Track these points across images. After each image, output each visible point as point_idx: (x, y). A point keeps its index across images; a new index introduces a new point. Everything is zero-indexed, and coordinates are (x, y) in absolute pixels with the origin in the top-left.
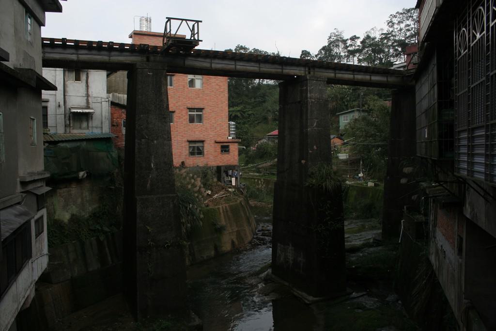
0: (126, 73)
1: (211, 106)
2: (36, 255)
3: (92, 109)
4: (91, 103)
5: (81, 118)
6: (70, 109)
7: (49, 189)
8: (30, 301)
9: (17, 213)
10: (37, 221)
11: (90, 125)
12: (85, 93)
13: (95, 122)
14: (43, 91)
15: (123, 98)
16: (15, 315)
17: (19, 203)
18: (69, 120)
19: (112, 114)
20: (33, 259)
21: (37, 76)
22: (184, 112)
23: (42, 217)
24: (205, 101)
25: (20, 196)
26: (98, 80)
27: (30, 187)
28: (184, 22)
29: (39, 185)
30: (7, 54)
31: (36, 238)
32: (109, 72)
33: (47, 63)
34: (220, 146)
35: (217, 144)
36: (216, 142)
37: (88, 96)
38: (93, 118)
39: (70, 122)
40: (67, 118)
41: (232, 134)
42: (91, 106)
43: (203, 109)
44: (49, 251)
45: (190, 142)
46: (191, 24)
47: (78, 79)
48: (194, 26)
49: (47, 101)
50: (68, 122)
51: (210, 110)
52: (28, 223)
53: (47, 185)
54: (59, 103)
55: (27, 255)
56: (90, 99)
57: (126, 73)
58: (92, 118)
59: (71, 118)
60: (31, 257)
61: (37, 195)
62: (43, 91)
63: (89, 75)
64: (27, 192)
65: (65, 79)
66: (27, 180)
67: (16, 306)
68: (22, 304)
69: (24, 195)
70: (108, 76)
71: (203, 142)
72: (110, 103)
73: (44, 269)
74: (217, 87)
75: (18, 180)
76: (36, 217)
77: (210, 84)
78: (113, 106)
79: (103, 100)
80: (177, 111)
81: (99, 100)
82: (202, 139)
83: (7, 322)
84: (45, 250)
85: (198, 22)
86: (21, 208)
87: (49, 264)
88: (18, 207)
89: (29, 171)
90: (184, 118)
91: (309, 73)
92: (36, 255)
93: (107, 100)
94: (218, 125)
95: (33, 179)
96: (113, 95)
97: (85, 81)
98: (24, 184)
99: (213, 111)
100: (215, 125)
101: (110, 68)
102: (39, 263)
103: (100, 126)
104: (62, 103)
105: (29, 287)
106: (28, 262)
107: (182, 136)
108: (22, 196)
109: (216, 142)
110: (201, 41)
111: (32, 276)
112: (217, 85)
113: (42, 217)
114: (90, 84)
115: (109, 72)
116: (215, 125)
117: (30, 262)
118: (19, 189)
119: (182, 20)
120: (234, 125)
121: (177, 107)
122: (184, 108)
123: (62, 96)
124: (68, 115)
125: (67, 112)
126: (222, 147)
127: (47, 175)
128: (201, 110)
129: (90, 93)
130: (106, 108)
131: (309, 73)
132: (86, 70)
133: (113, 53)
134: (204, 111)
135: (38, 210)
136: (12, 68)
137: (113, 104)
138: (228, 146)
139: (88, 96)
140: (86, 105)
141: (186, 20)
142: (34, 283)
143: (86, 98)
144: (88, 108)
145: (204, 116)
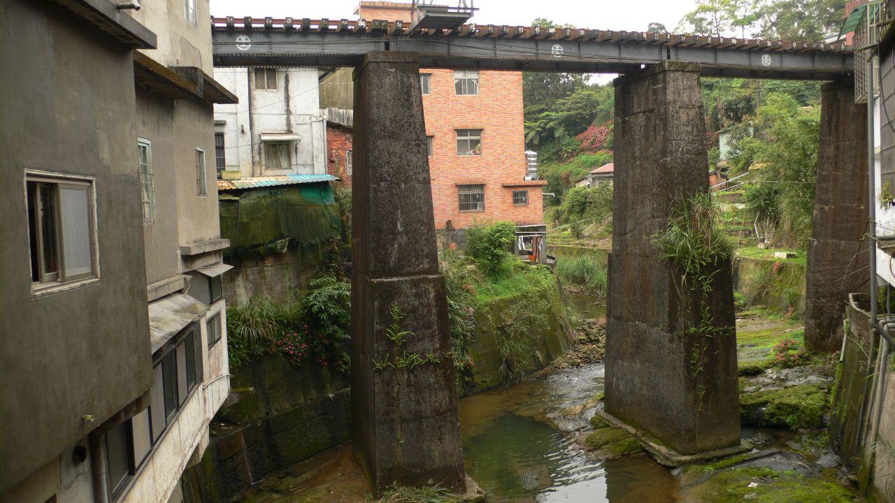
0: (350, 70)
1: (494, 126)
2: (210, 377)
3: (297, 134)
5: (278, 150)
6: (260, 136)
7: (228, 267)
8: (202, 452)
9: (177, 307)
10: (210, 322)
11: (294, 161)
12: (285, 108)
13: (301, 157)
14: (215, 105)
15: (347, 114)
16: (179, 476)
17: (180, 292)
18: (260, 153)
19: (329, 142)
20: (206, 382)
21: (204, 80)
22: (449, 136)
23: (218, 314)
24: (485, 117)
25: (182, 281)
26: (305, 85)
27: (198, 265)
29: (212, 260)
30: (154, 36)
31: (209, 349)
32: (322, 73)
33: (221, 61)
34: (511, 193)
35: (505, 191)
36: (505, 187)
37: (288, 112)
38: (299, 150)
39: (260, 158)
40: (256, 152)
41: (532, 172)
42: (293, 129)
43: (481, 130)
44: (231, 371)
45: (460, 187)
47: (272, 85)
49: (222, 124)
50: (257, 158)
51: (494, 131)
52: (194, 324)
53: (225, 262)
54: (242, 126)
55: (195, 376)
56: (292, 118)
57: (350, 70)
58: (296, 150)
59: (263, 151)
60: (202, 380)
61: (209, 278)
62: (215, 105)
63: (290, 78)
64: (195, 273)
65: (252, 86)
66: (192, 254)
67: (179, 462)
68: (188, 458)
69: (189, 277)
70: (321, 78)
71: (482, 186)
72: (325, 124)
73: (223, 400)
74: (505, 92)
75: (179, 252)
76: (209, 314)
77: (493, 87)
78: (330, 129)
79: (314, 119)
80: (438, 135)
81: (307, 119)
82: (480, 182)
83: (165, 488)
84: (225, 370)
86: (184, 300)
87: (231, 393)
88: (179, 297)
89: (194, 237)
90: (449, 146)
91: (669, 57)
92: (210, 377)
93: (321, 119)
94: (507, 157)
95: (202, 252)
96: (330, 112)
98: (188, 258)
99: (498, 134)
100: (503, 158)
101: (325, 65)
102: (213, 392)
103: (309, 162)
105: (200, 430)
106: (197, 388)
107: (447, 177)
108: (185, 279)
109: (505, 187)
111: (205, 411)
112: (504, 88)
113: (218, 314)
114: (291, 94)
115: (322, 73)
116: (503, 158)
117: (201, 388)
118: (180, 267)
120: (534, 156)
121: (437, 128)
122: (450, 130)
125: (257, 141)
126: (515, 195)
127: (226, 244)
128: (478, 131)
129: (292, 109)
130: (319, 131)
131: (669, 57)
132: (286, 70)
133: (328, 39)
134: (483, 135)
135: (212, 303)
136: (166, 66)
137: (331, 126)
138: (525, 193)
139: (288, 112)
140: (286, 128)
142: (207, 424)
143: (285, 116)
144: (289, 132)
145: (483, 141)
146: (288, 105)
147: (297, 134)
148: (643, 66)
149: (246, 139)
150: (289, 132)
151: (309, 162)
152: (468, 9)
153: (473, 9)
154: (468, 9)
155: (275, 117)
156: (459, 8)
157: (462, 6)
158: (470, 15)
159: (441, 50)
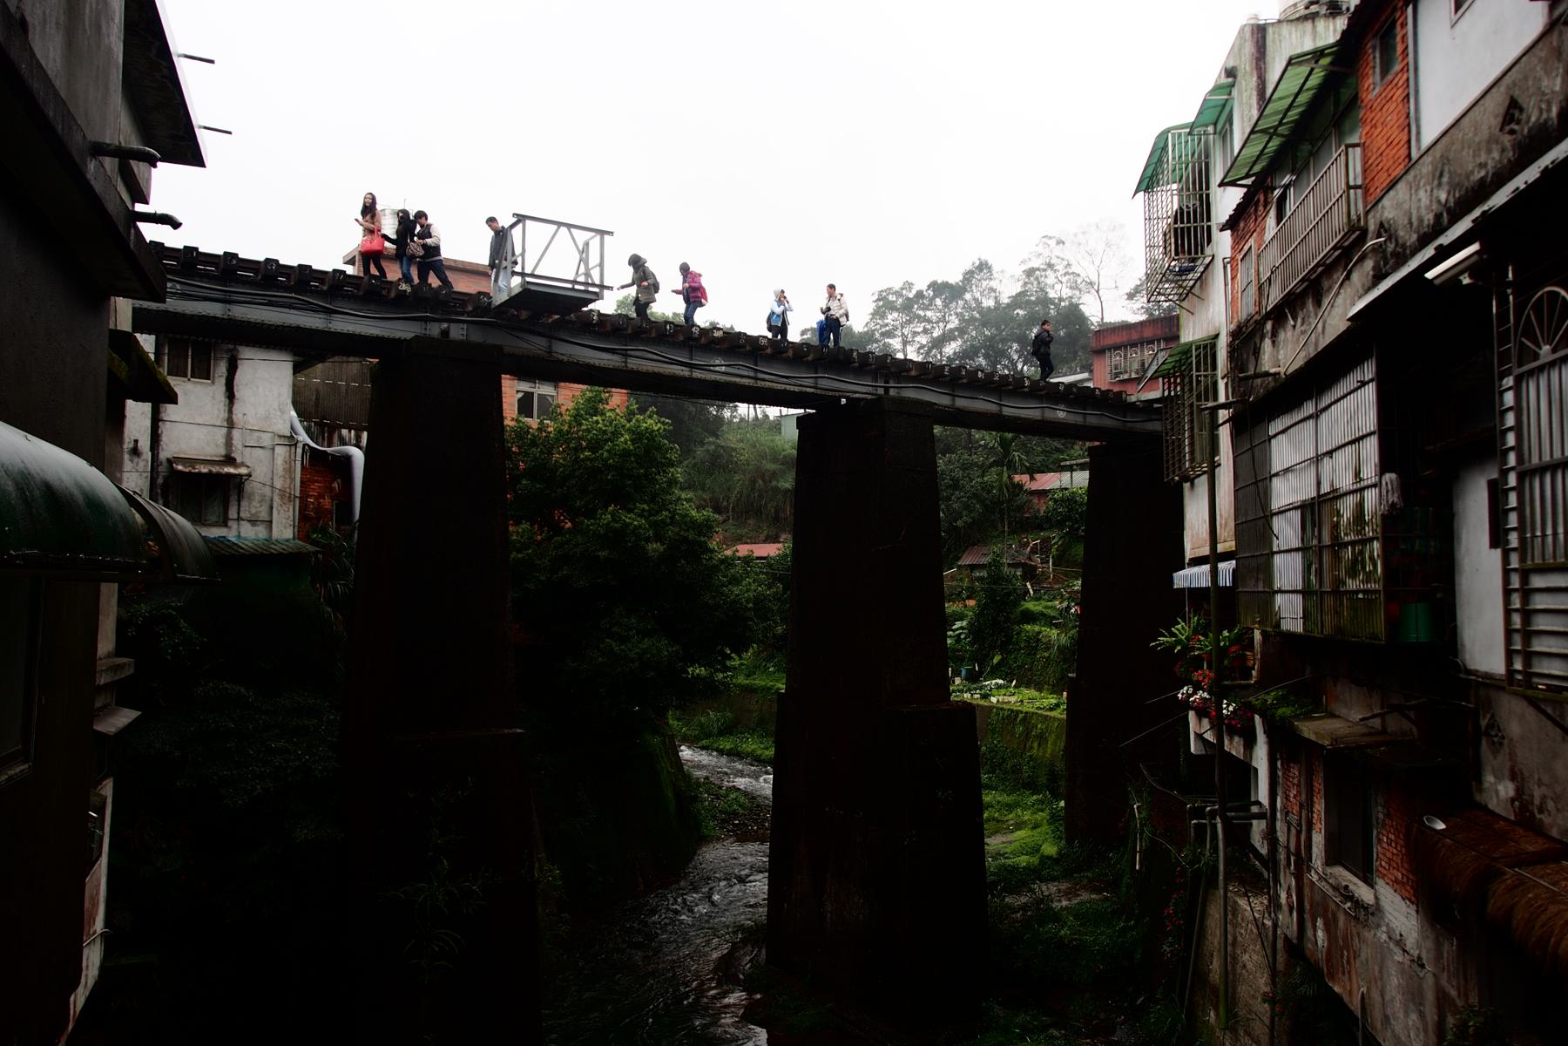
3: (243, 464)
4: (240, 446)
11: (233, 513)
13: (251, 508)
14: (129, 403)
28: (563, 230)
37: (231, 424)
46: (582, 237)
47: (203, 373)
48: (587, 244)
54: (136, 441)
56: (236, 434)
62: (129, 403)
70: (297, 369)
72: (299, 451)
81: (266, 440)
85: (602, 233)
97: (223, 381)
101: (304, 349)
103: (264, 515)
104: (145, 444)
110: (677, 292)
119: (560, 224)
123: (148, 423)
124: (160, 481)
139: (231, 424)
141: (569, 226)
146: (230, 411)
147: (243, 464)
148: (844, 401)
149: (142, 464)
150: (229, 460)
151: (264, 515)
152: (594, 285)
153: (602, 287)
154: (594, 285)
155: (204, 430)
156: (575, 282)
157: (581, 279)
158: (598, 296)
159: (535, 345)
